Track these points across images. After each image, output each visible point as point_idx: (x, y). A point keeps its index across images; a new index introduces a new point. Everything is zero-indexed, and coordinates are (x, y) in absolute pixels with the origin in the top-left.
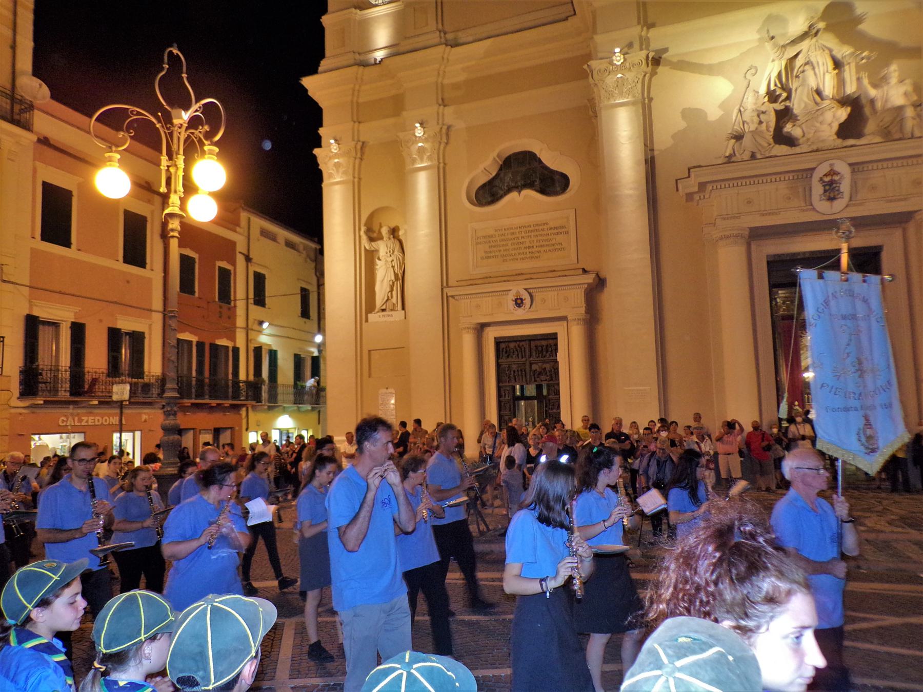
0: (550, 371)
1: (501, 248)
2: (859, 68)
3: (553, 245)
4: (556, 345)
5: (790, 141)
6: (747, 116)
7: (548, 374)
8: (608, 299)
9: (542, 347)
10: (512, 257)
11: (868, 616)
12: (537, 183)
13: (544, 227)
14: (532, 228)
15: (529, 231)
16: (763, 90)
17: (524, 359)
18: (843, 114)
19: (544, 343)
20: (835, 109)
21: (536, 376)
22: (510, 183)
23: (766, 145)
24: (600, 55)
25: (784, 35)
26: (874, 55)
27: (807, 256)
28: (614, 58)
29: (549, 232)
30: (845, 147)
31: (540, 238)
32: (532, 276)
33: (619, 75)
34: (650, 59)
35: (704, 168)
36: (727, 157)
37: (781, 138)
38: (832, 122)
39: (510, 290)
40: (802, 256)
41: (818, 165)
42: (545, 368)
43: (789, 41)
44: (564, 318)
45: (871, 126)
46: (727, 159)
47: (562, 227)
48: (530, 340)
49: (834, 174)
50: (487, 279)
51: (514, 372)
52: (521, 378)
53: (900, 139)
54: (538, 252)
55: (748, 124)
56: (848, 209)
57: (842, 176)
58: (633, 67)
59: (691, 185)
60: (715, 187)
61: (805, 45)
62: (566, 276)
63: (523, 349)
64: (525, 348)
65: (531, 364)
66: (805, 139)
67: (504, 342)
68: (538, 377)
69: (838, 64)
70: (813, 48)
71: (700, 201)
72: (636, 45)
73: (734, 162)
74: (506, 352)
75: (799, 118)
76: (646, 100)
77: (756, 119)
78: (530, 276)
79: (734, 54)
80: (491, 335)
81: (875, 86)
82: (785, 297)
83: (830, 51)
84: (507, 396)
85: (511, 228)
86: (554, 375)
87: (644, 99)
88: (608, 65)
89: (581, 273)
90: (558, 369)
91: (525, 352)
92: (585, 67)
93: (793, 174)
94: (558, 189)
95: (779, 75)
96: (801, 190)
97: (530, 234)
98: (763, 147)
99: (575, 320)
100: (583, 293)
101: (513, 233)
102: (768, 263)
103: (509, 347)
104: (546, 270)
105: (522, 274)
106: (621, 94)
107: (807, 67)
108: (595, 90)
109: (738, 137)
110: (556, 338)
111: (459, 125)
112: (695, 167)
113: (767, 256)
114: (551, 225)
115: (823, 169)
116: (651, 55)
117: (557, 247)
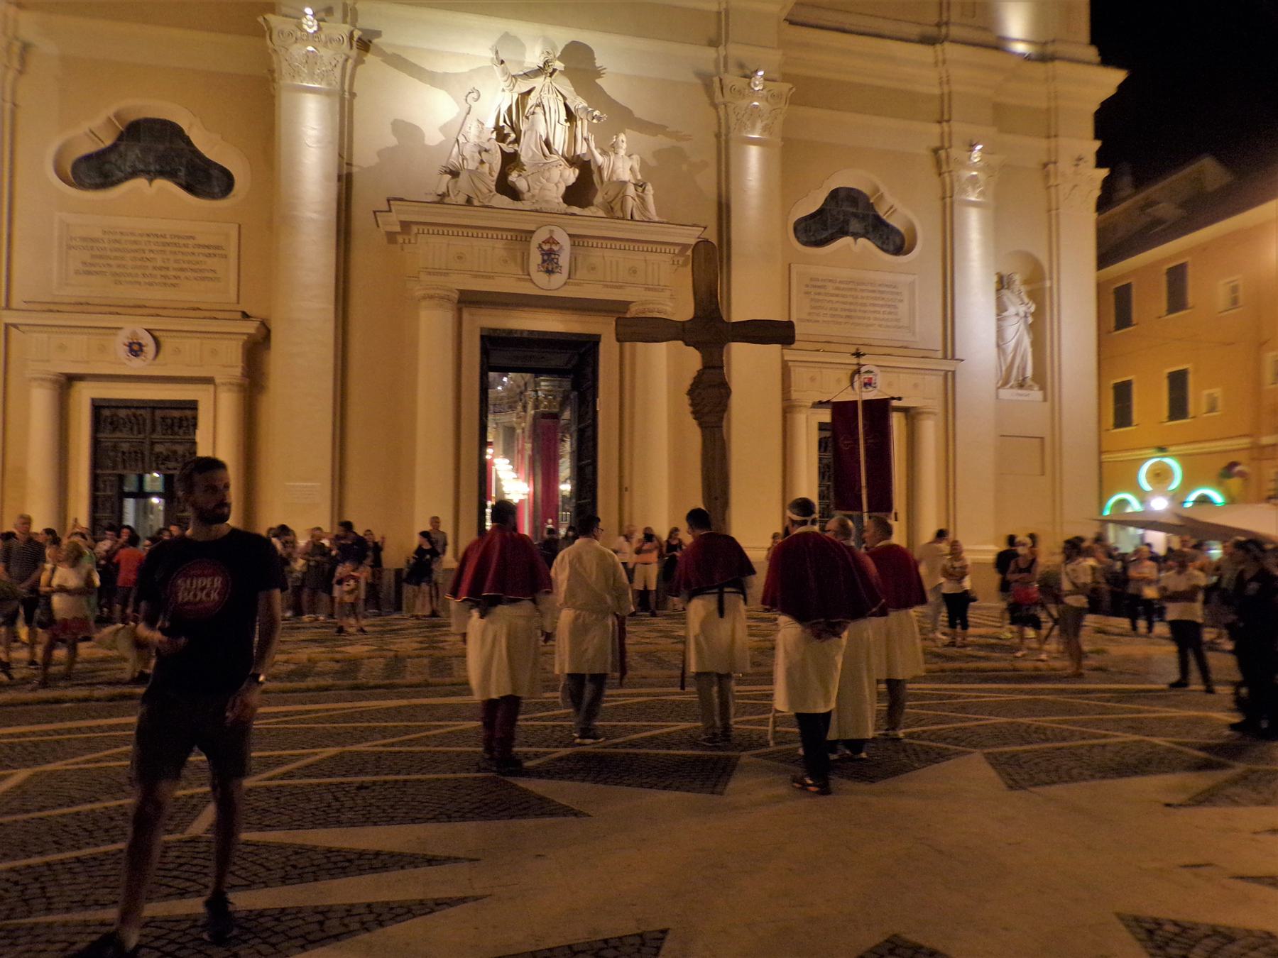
1: (111, 262)
2: (591, 128)
3: (201, 270)
4: (195, 418)
5: (514, 194)
6: (469, 151)
7: (180, 460)
8: (278, 361)
9: (173, 419)
12: (182, 174)
14: (168, 240)
15: (164, 244)
16: (490, 124)
17: (142, 436)
18: (571, 175)
19: (176, 414)
22: (137, 163)
23: (485, 191)
24: (285, 10)
25: (521, 63)
27: (525, 335)
28: (304, 21)
29: (197, 250)
30: (566, 214)
31: (180, 257)
33: (310, 48)
34: (355, 39)
35: (408, 203)
36: (439, 195)
37: (505, 188)
38: (559, 182)
41: (538, 228)
43: (522, 73)
44: (209, 381)
45: (598, 199)
46: (439, 198)
47: (217, 247)
48: (154, 408)
50: (82, 306)
53: (618, 218)
54: (175, 277)
55: (466, 159)
56: (567, 287)
57: (561, 248)
58: (331, 42)
59: (392, 222)
60: (421, 231)
61: (539, 82)
63: (141, 422)
65: (153, 444)
68: (163, 464)
69: (570, 116)
70: (547, 89)
72: (338, 14)
74: (111, 423)
75: (525, 168)
76: (347, 93)
79: (464, 69)
80: (84, 396)
81: (604, 153)
82: (548, 391)
83: (564, 98)
85: (132, 234)
88: (294, 28)
92: (260, 19)
93: (512, 234)
94: (217, 190)
95: (510, 109)
96: (519, 254)
98: (480, 191)
101: (135, 242)
102: (482, 337)
103: (117, 416)
104: (187, 305)
105: (145, 307)
106: (312, 76)
107: (539, 110)
108: (274, 57)
109: (455, 174)
111: (47, 47)
113: (482, 329)
114: (201, 240)
116: (357, 34)
117: (207, 275)
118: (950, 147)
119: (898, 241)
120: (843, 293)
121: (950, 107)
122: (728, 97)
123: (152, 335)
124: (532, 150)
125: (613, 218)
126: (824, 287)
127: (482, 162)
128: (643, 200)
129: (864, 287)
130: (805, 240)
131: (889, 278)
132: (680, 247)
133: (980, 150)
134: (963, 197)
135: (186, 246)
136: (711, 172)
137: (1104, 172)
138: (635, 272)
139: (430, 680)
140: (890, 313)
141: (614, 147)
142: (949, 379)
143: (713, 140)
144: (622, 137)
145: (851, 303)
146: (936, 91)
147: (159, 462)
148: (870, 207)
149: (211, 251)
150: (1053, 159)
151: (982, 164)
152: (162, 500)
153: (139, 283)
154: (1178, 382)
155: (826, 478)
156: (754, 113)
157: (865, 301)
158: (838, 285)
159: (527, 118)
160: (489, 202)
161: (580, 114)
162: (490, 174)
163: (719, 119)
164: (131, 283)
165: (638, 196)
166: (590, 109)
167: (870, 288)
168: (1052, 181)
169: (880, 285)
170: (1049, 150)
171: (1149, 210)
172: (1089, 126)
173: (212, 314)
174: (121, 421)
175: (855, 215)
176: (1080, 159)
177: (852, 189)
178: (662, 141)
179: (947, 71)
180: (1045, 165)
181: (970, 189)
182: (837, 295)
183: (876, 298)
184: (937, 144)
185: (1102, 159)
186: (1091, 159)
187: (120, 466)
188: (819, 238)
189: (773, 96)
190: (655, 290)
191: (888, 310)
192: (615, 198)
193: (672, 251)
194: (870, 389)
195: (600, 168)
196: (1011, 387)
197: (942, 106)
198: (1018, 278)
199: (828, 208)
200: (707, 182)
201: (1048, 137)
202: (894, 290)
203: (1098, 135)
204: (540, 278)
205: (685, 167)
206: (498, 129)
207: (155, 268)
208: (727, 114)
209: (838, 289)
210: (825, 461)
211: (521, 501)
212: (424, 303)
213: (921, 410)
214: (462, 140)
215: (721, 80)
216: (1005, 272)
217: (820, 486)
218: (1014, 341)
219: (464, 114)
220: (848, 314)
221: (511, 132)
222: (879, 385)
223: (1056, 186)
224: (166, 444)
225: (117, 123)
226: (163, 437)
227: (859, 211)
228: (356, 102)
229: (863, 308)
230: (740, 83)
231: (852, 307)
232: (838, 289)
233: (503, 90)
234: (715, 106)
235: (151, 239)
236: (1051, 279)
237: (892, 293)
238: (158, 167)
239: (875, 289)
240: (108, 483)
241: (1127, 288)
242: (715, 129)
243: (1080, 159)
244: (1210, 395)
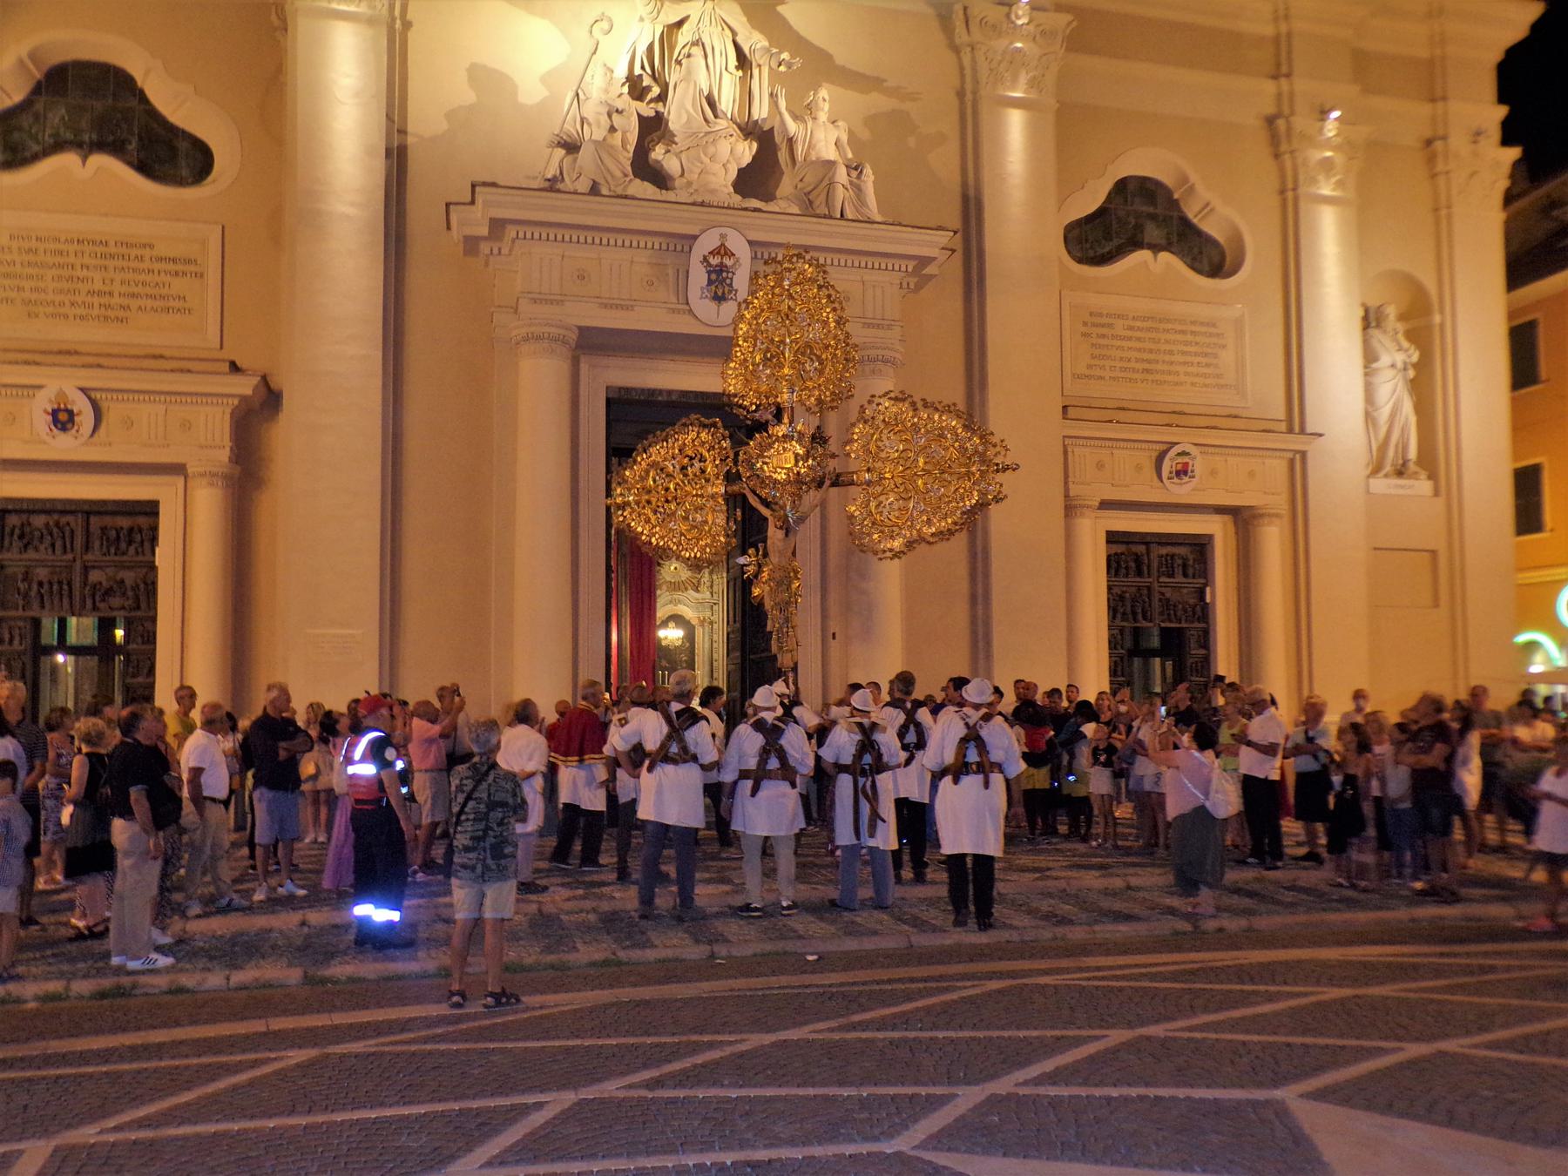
0: (135, 588)
2: (774, 76)
3: (162, 297)
4: (154, 529)
5: (659, 178)
6: (590, 110)
7: (130, 593)
9: (118, 531)
10: (50, 310)
11: (720, 1038)
12: (133, 146)
13: (139, 252)
14: (113, 250)
15: (104, 256)
16: (621, 72)
17: (70, 556)
18: (746, 151)
19: (124, 522)
20: (733, 139)
21: (97, 598)
23: (618, 174)
27: (674, 398)
29: (157, 266)
31: (130, 276)
32: (102, 361)
37: (645, 168)
39: (40, 387)
42: (122, 581)
44: (178, 469)
45: (786, 186)
47: (189, 261)
48: (88, 513)
49: (726, 254)
51: (40, 584)
52: (56, 601)
53: (825, 217)
55: (589, 124)
59: (475, 221)
60: (521, 235)
62: (189, 371)
63: (67, 534)
64: (72, 531)
65: (86, 569)
67: (16, 511)
68: (104, 600)
69: (743, 61)
71: (491, 258)
73: (559, 191)
74: (21, 537)
76: (398, 22)
78: (98, 360)
81: (796, 118)
83: (734, 33)
84: (16, 642)
86: (142, 598)
87: (393, 19)
89: (227, 369)
90: (154, 583)
91: (72, 537)
94: (185, 172)
95: (650, 48)
96: (671, 271)
97: (107, 263)
98: (613, 176)
99: (203, 475)
100: (227, 417)
101: (61, 253)
102: (609, 401)
105: (76, 353)
107: (697, 51)
109: (571, 147)
110: (157, 514)
112: (485, 184)
114: (162, 250)
117: (171, 303)
118: (1292, 113)
119: (1216, 259)
120: (1139, 334)
121: (1289, 52)
122: (977, 35)
123: (89, 398)
124: (687, 112)
126: (1110, 326)
128: (858, 190)
129: (1170, 326)
131: (1203, 312)
132: (915, 263)
133: (1336, 119)
134: (1313, 190)
135: (141, 259)
136: (953, 147)
137: (1514, 153)
139: (622, 955)
140: (1207, 365)
141: (810, 108)
142: (1298, 465)
143: (955, 102)
144: (823, 93)
145: (1151, 351)
146: (1268, 30)
147: (95, 599)
148: (1174, 204)
149: (179, 267)
150: (1441, 132)
151: (1339, 140)
152: (71, 659)
153: (66, 317)
155: (1119, 616)
156: (1015, 60)
157: (1168, 347)
158: (1131, 323)
159: (679, 63)
160: (625, 188)
161: (757, 59)
163: (962, 69)
164: (53, 316)
166: (775, 50)
167: (1179, 328)
168: (1440, 167)
169: (1193, 323)
171: (1555, 213)
172: (1488, 85)
173: (184, 365)
174: (37, 534)
175: (1153, 217)
176: (1478, 133)
177: (1145, 179)
178: (879, 102)
181: (1321, 178)
182: (1130, 339)
183: (1187, 343)
184: (1270, 110)
185: (1509, 135)
186: (1495, 133)
187: (36, 604)
188: (1100, 251)
189: (1043, 33)
190: (878, 326)
191: (1204, 360)
193: (903, 269)
194: (1186, 479)
195: (791, 142)
196: (1386, 476)
197: (1277, 55)
198: (1391, 311)
199: (1112, 206)
200: (945, 162)
201: (1433, 100)
202: (1212, 330)
203: (1502, 98)
204: (704, 307)
205: (912, 142)
207: (90, 293)
208: (974, 61)
209: (1131, 328)
210: (1116, 590)
213: (1261, 512)
214: (581, 96)
215: (965, 9)
216: (1373, 303)
217: (1110, 627)
218: (1391, 404)
219: (589, 55)
220: (1147, 366)
221: (653, 84)
222: (1197, 473)
223: (1447, 173)
224: (108, 570)
225: (31, 67)
226: (104, 558)
227: (1159, 211)
228: (411, 35)
229: (1167, 358)
230: (995, 13)
231: (1152, 356)
232: (1131, 328)
233: (642, 19)
234: (956, 50)
235: (88, 248)
236: (1442, 312)
237: (1211, 335)
238: (94, 137)
239: (1184, 328)
240: (16, 632)
241: (1532, 325)
243: (1478, 133)
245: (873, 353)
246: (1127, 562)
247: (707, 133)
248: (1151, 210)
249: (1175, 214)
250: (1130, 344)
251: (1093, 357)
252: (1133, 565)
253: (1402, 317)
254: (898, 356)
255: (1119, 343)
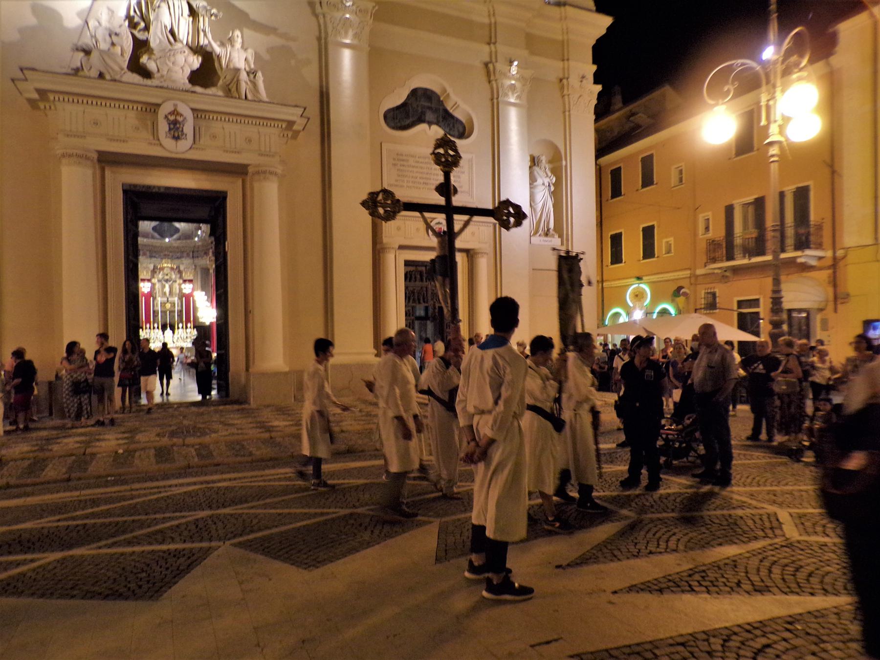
5: (146, 73)
16: (122, 13)
18: (196, 62)
26: (221, 15)
27: (162, 190)
37: (136, 66)
40: (157, 190)
41: (163, 102)
45: (221, 82)
56: (192, 151)
57: (185, 118)
60: (57, 99)
66: (159, 75)
69: (193, 12)
77: (108, 38)
81: (222, 44)
96: (149, 123)
102: (125, 192)
109: (87, 52)
112: (28, 69)
113: (123, 185)
115: (166, 108)
118: (496, 61)
120: (421, 165)
124: (160, 39)
125: (232, 97)
127: (113, 44)
128: (255, 85)
130: (393, 124)
134: (506, 99)
137: (599, 88)
138: (250, 141)
141: (231, 41)
143: (315, 43)
145: (427, 174)
146: (486, 21)
148: (441, 103)
150: (566, 76)
151: (518, 76)
154: (648, 233)
158: (417, 159)
160: (121, 76)
161: (201, 12)
162: (122, 55)
163: (319, 26)
165: (250, 81)
168: (565, 92)
170: (564, 68)
171: (632, 119)
175: (430, 108)
176: (583, 77)
177: (425, 91)
179: (493, 7)
180: (561, 80)
181: (510, 93)
184: (487, 59)
185: (597, 80)
186: (591, 78)
188: (403, 124)
192: (231, 82)
198: (544, 159)
200: (311, 74)
201: (563, 60)
203: (594, 62)
204: (169, 143)
205: (293, 62)
206: (129, 17)
209: (418, 162)
211: (212, 323)
212: (64, 161)
216: (536, 154)
220: (425, 181)
229: (435, 177)
232: (418, 162)
234: (316, 16)
241: (619, 169)
242: (317, 33)
243: (583, 77)
244: (667, 242)
245: (264, 169)
246: (415, 275)
247: (170, 50)
248: (427, 104)
249: (441, 108)
250: (415, 170)
251: (399, 176)
252: (418, 276)
253: (550, 162)
254: (279, 171)
255: (411, 169)
